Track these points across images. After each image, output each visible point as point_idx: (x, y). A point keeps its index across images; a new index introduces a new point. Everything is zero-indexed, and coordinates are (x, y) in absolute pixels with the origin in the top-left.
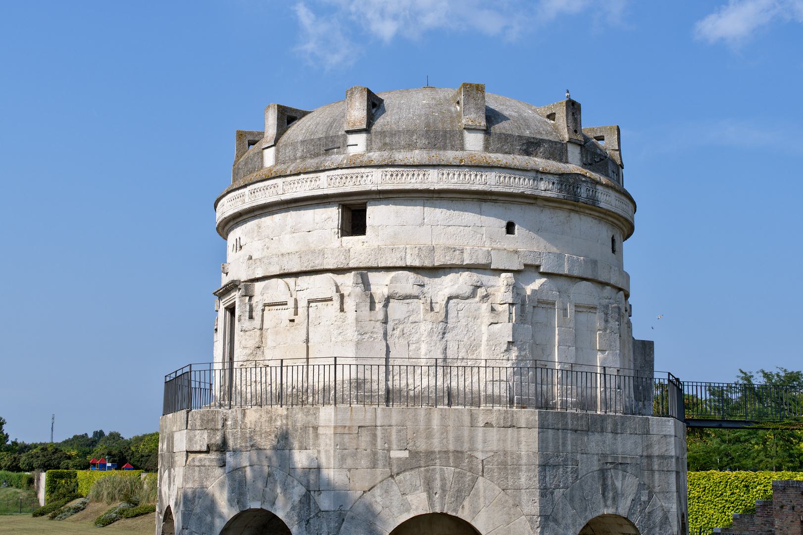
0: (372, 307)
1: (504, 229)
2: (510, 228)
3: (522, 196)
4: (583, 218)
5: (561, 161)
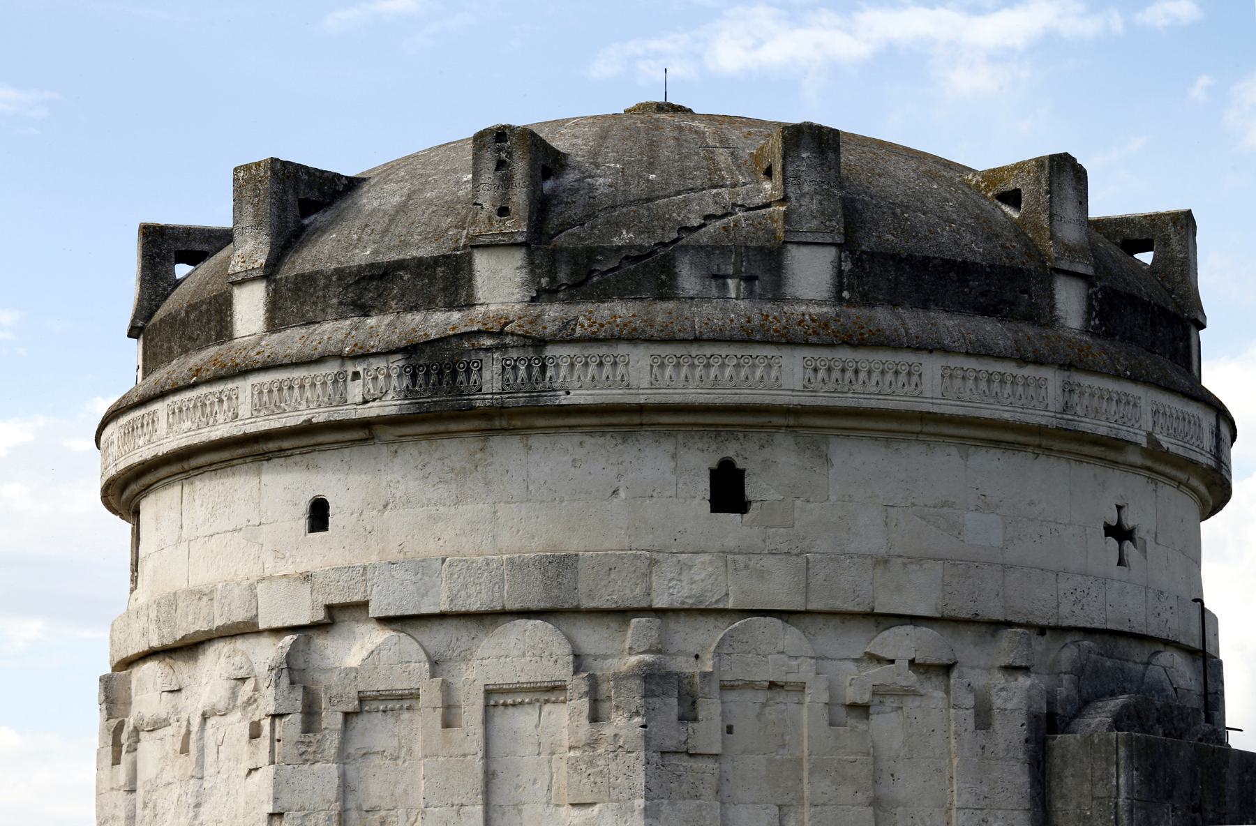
0: (116, 761)
1: (303, 523)
2: (319, 515)
3: (308, 429)
4: (537, 441)
5: (450, 306)
